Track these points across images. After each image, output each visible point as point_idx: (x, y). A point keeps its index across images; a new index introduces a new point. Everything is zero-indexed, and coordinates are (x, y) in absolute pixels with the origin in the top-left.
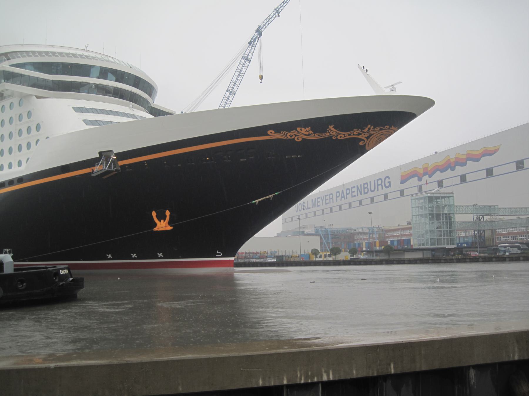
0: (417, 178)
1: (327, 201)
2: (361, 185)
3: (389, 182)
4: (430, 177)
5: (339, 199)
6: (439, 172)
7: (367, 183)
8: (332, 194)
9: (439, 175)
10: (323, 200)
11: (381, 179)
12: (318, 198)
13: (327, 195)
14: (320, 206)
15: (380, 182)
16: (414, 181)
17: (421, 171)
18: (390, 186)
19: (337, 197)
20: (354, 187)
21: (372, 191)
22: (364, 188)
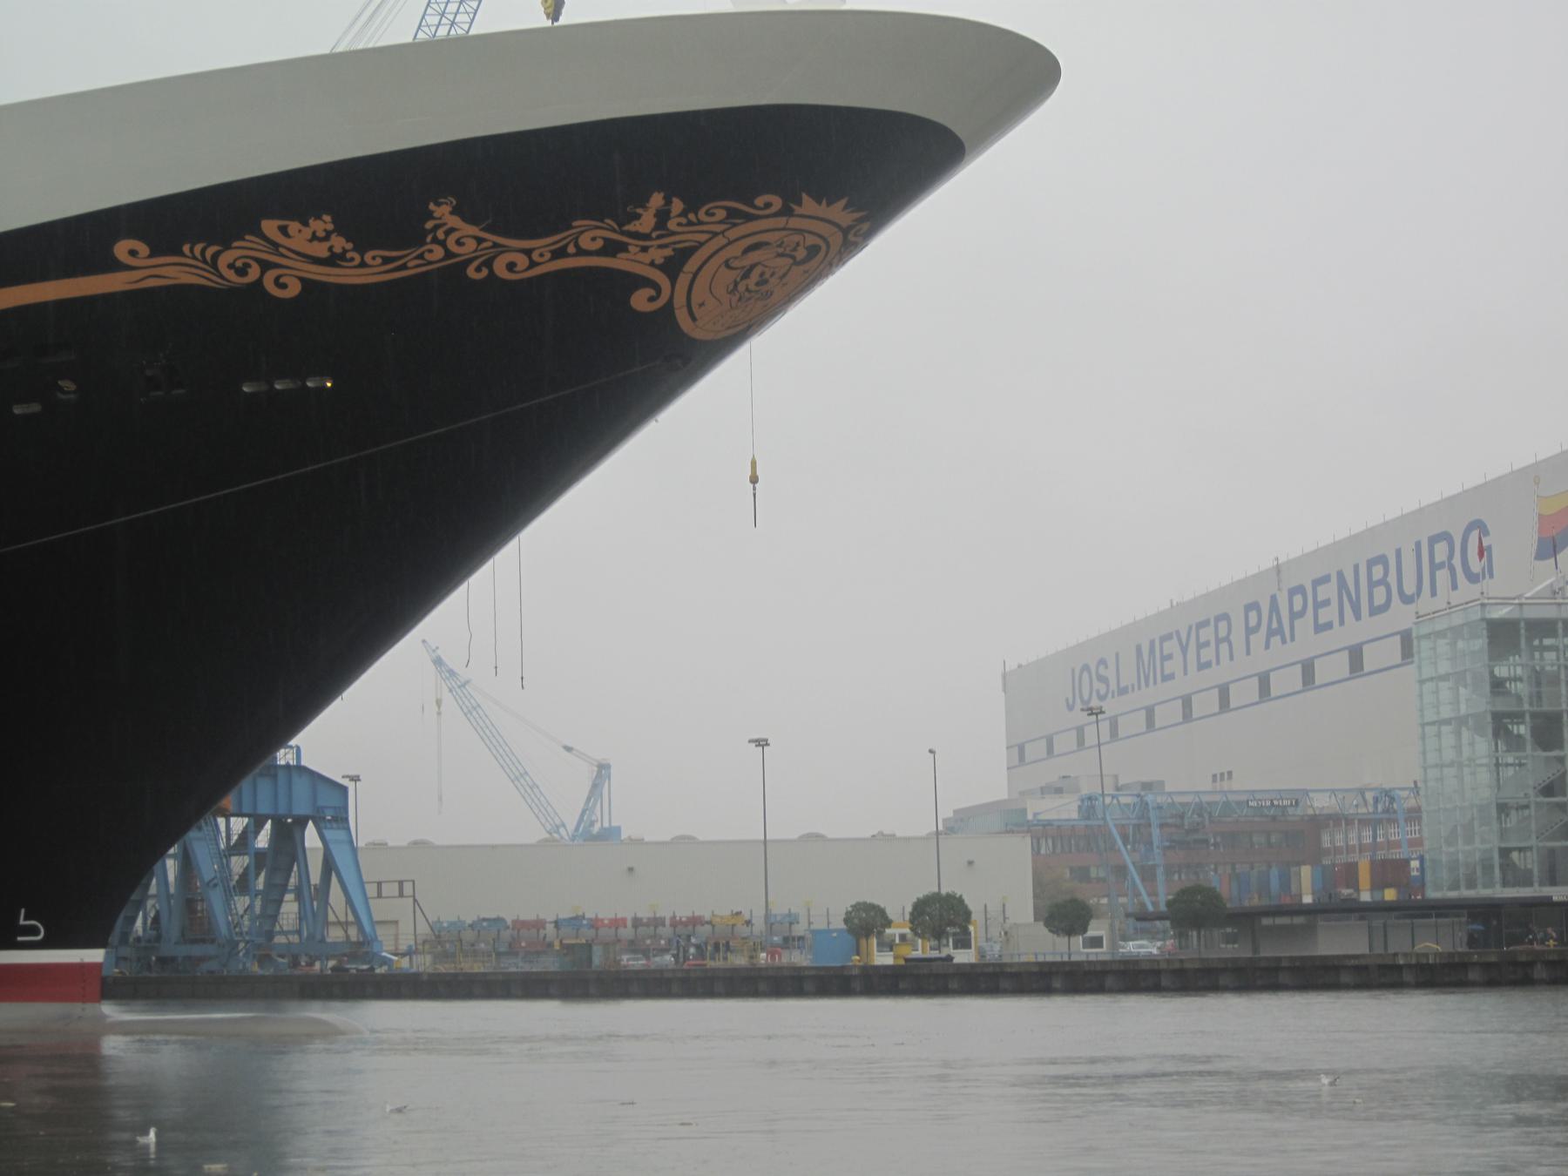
1: (1208, 654)
2: (1356, 568)
5: (1258, 639)
7: (1382, 560)
8: (1225, 617)
10: (1184, 650)
11: (1446, 537)
12: (1164, 639)
13: (1205, 624)
14: (1171, 677)
19: (1250, 631)
20: (1325, 579)
21: (1407, 600)
22: (1372, 585)
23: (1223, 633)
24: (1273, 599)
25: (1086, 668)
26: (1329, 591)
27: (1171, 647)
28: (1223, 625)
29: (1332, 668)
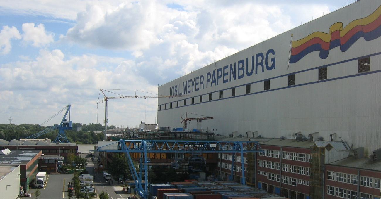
0: (318, 52)
1: (198, 86)
2: (235, 63)
3: (273, 60)
4: (343, 49)
6: (362, 39)
7: (242, 61)
8: (202, 76)
9: (361, 47)
10: (193, 85)
11: (261, 54)
15: (260, 59)
16: (313, 59)
17: (327, 39)
18: (273, 66)
19: (208, 81)
21: (249, 74)
22: (239, 69)
23: (202, 81)
24: (214, 72)
25: (173, 87)
26: (227, 70)
27: (190, 84)
28: (202, 78)
29: (227, 93)
